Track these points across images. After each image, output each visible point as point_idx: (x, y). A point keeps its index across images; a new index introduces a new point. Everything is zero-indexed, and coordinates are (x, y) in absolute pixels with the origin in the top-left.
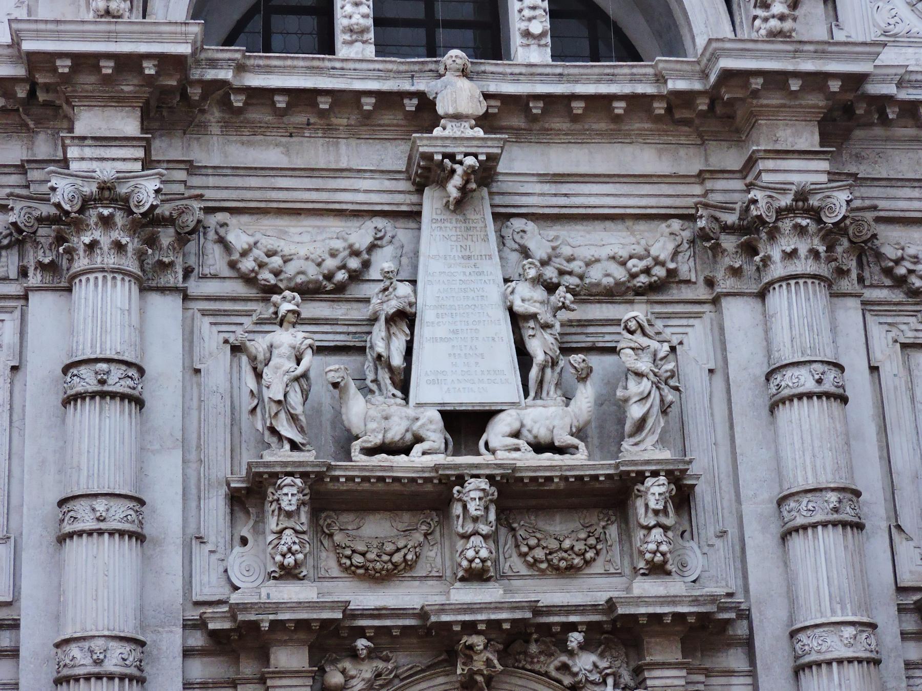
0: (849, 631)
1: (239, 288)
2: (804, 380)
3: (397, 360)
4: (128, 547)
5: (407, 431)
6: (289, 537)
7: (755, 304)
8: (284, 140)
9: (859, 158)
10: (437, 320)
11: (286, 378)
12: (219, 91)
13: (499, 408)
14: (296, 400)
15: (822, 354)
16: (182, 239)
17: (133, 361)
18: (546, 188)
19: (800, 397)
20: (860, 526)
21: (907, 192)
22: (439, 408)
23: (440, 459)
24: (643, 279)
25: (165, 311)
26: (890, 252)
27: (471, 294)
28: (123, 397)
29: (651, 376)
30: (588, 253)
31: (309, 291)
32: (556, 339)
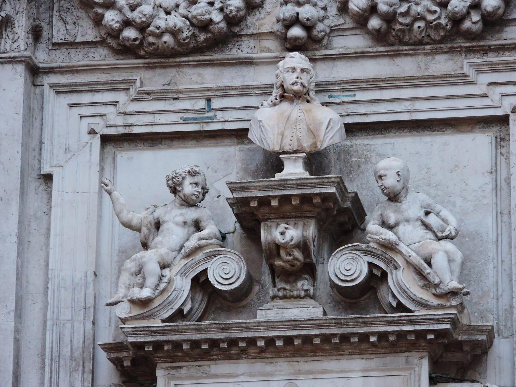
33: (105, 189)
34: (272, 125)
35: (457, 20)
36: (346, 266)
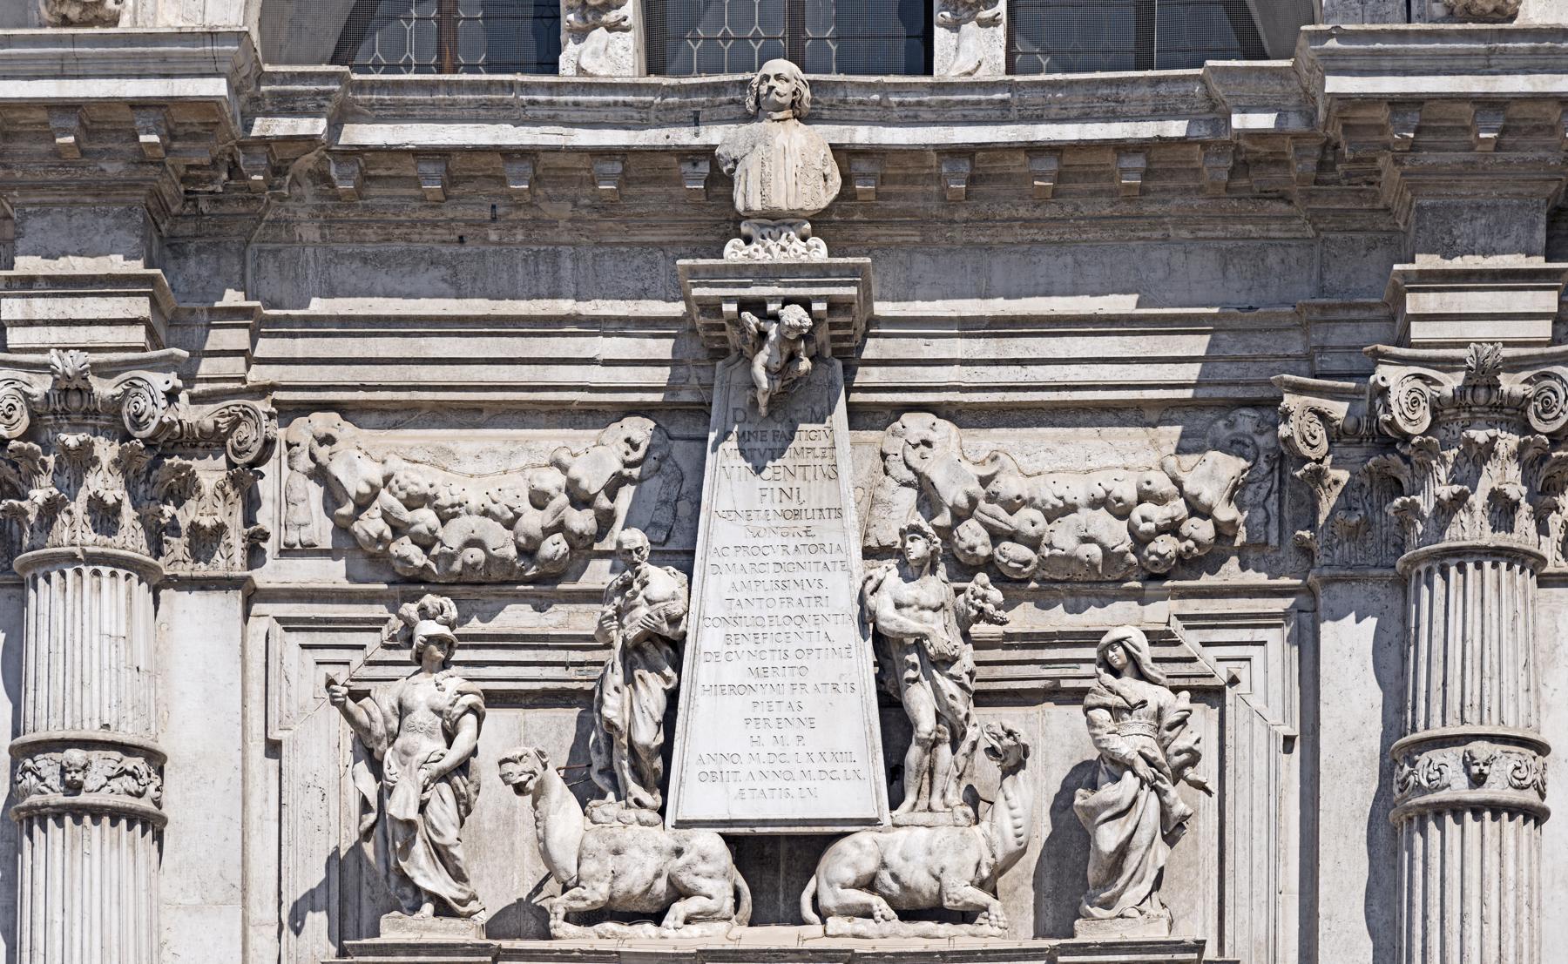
3: (647, 735)
5: (658, 875)
8: (446, 250)
10: (726, 649)
11: (422, 776)
13: (839, 829)
14: (444, 817)
15: (1495, 719)
17: (136, 741)
19: (1439, 811)
22: (722, 830)
24: (1166, 545)
27: (796, 593)
28: (116, 815)
29: (1141, 765)
30: (1048, 494)
31: (483, 584)
32: (962, 686)
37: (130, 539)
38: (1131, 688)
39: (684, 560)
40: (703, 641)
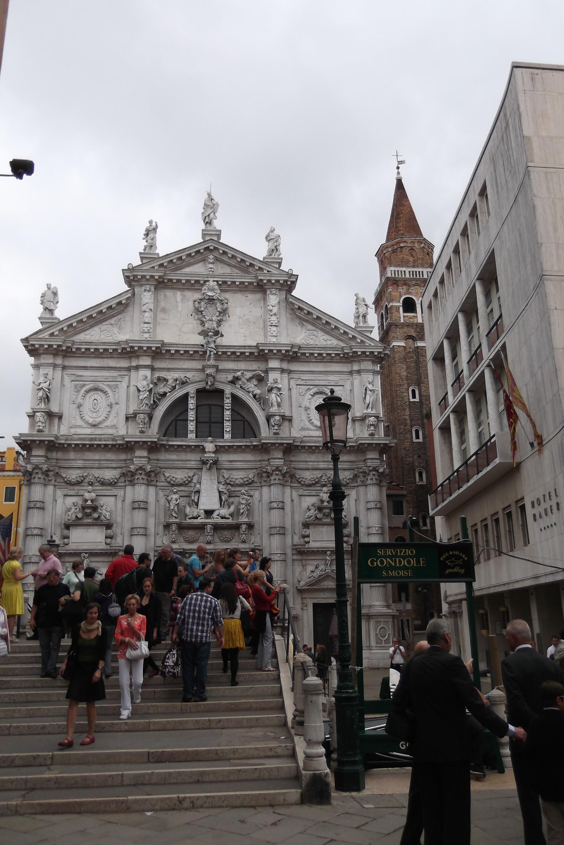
0: (279, 555)
1: (166, 484)
2: (275, 505)
3: (196, 501)
4: (143, 537)
6: (174, 535)
7: (268, 487)
9: (293, 456)
12: (164, 445)
16: (156, 475)
18: (229, 463)
20: (284, 534)
21: (302, 463)
23: (203, 521)
24: (246, 482)
25: (152, 490)
26: (298, 476)
30: (236, 477)
33: (64, 503)
34: (87, 496)
35: (111, 483)
36: (96, 515)
37: (145, 482)
38: (244, 496)
39: (200, 483)
40: (202, 491)
